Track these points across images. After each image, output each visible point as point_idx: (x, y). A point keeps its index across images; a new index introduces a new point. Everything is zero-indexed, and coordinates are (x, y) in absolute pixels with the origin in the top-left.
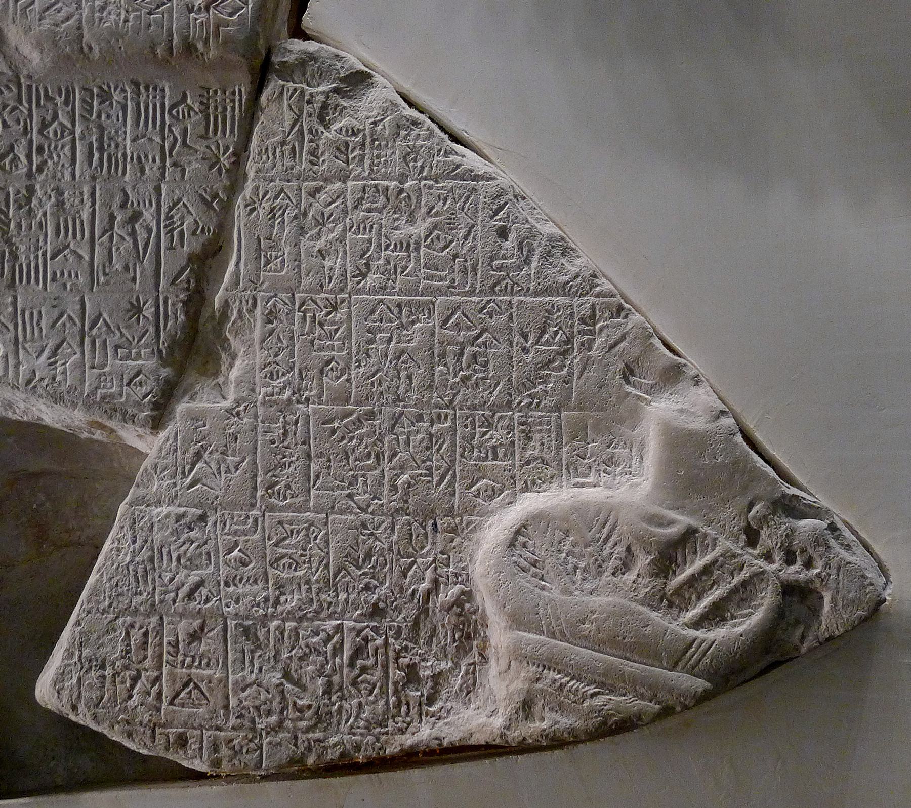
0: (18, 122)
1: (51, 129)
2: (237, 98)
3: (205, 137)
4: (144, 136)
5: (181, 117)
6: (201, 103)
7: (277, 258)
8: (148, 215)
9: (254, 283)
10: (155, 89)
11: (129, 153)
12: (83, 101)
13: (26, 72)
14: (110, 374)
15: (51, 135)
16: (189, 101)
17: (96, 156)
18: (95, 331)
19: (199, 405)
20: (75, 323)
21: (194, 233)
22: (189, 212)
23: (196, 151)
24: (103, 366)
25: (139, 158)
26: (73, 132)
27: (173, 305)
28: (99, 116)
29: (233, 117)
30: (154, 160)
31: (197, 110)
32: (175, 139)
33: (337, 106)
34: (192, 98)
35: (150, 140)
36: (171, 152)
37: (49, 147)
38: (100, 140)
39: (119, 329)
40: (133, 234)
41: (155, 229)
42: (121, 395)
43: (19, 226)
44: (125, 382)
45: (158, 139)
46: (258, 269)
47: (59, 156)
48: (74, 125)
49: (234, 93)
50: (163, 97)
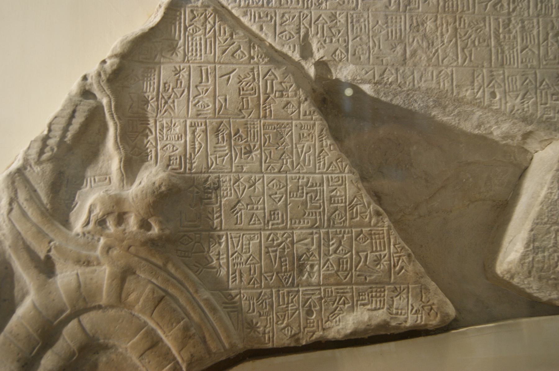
14: (550, 107)
18: (542, 87)
20: (532, 84)
24: (546, 104)
43: (505, 37)
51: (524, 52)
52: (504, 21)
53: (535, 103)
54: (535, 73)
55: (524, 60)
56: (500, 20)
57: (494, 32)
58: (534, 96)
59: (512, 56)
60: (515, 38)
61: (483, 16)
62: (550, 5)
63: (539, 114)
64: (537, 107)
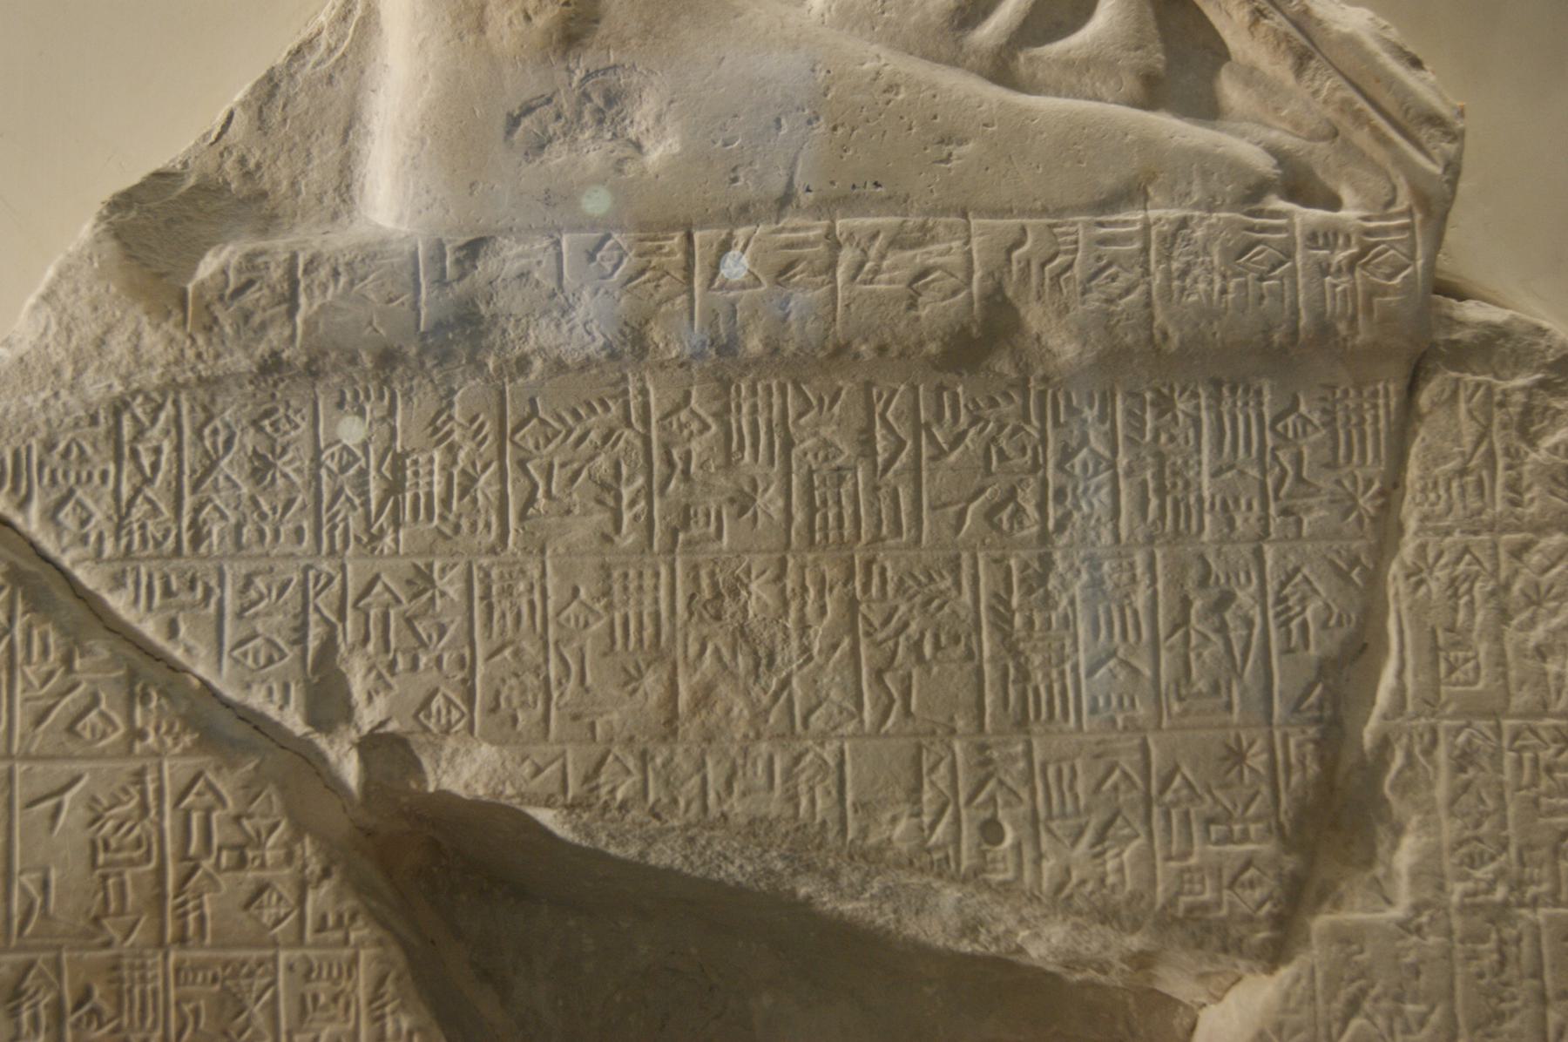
0: (1023, 450)
1: (1078, 460)
2: (1381, 401)
3: (1332, 465)
4: (1231, 467)
5: (1290, 434)
6: (1324, 411)
7: (1467, 660)
8: (1244, 597)
9: (1431, 702)
10: (1246, 391)
11: (1206, 494)
12: (1129, 413)
13: (1040, 372)
14: (1200, 869)
15: (1078, 470)
16: (1303, 409)
17: (1154, 503)
18: (1169, 796)
19: (1351, 916)
20: (1133, 785)
21: (1324, 625)
22: (1315, 591)
23: (1319, 490)
24: (1185, 855)
25: (1224, 503)
26: (1113, 466)
27: (1299, 745)
28: (1156, 438)
29: (1376, 433)
30: (1249, 507)
31: (1316, 422)
32: (1284, 472)
33: (1547, 408)
34: (1307, 402)
35: (1242, 473)
36: (1277, 490)
37: (1075, 489)
38: (1159, 475)
39: (1210, 792)
40: (1222, 629)
41: (1258, 620)
42: (1219, 905)
43: (1030, 623)
44: (1226, 880)
45: (1254, 472)
46: (1437, 681)
47: (1091, 505)
48: (1115, 452)
49: (1375, 394)
50: (1260, 404)
51: (1102, 671)
52: (1025, 566)
53: (1147, 856)
54: (1145, 750)
55: (1101, 702)
56: (1013, 562)
57: (991, 608)
58: (1142, 831)
59: (1056, 688)
60: (1067, 622)
61: (952, 552)
62: (1192, 500)
63: (1160, 896)
64: (1154, 866)
